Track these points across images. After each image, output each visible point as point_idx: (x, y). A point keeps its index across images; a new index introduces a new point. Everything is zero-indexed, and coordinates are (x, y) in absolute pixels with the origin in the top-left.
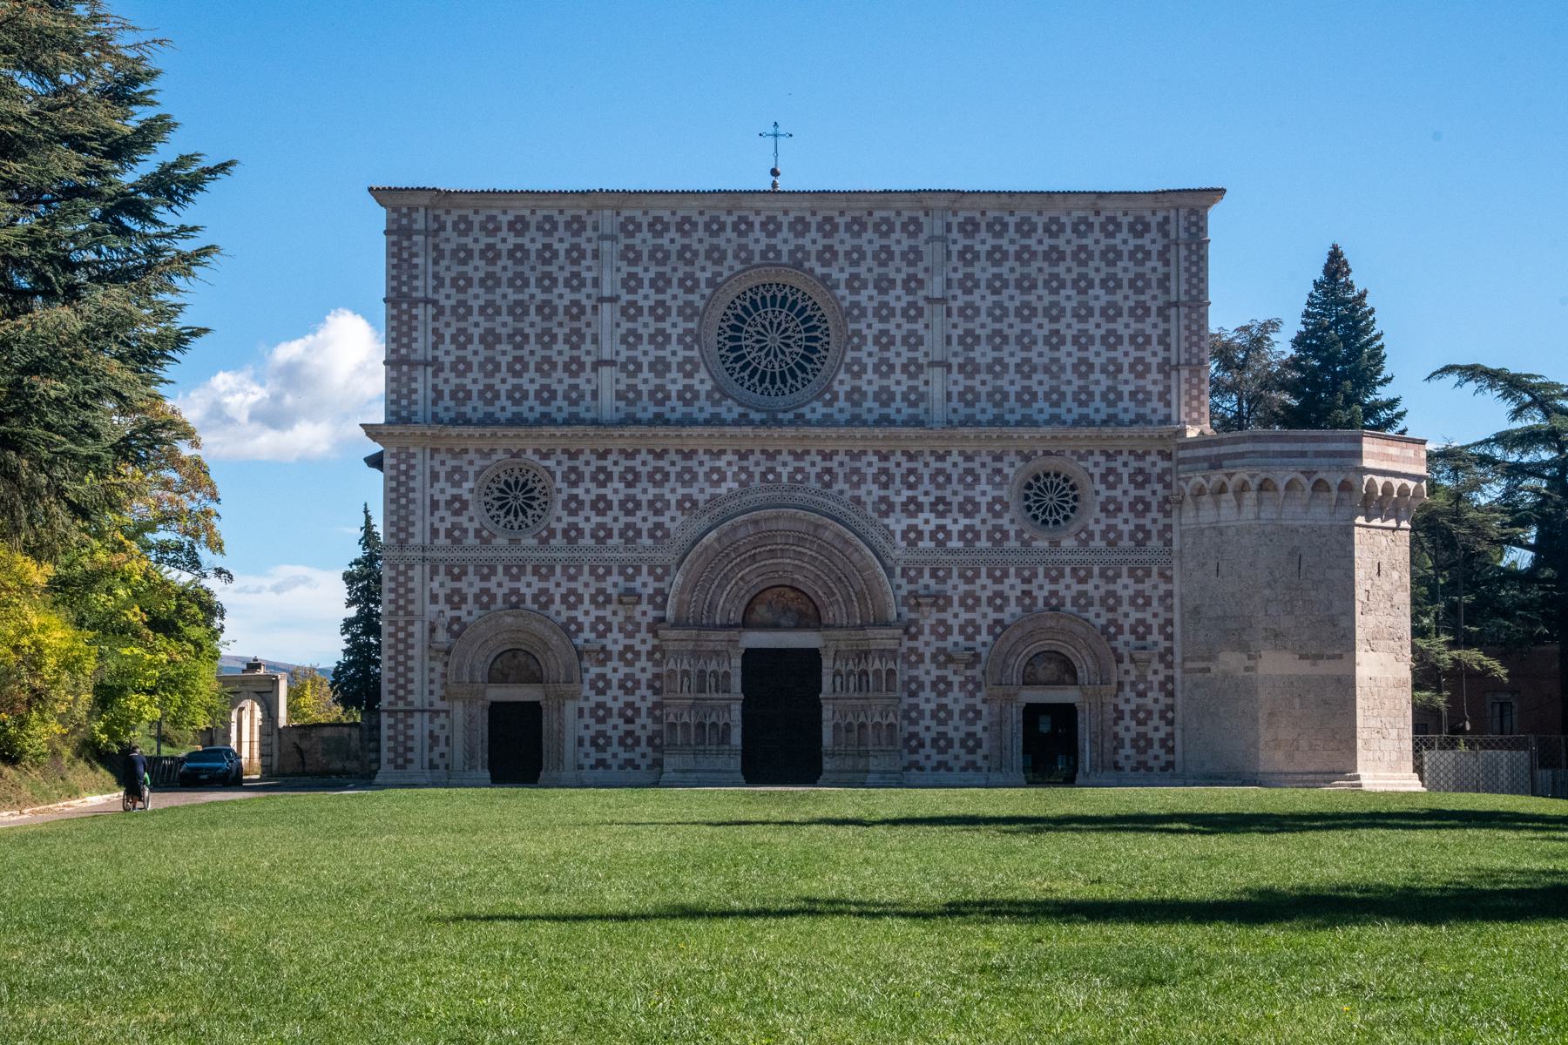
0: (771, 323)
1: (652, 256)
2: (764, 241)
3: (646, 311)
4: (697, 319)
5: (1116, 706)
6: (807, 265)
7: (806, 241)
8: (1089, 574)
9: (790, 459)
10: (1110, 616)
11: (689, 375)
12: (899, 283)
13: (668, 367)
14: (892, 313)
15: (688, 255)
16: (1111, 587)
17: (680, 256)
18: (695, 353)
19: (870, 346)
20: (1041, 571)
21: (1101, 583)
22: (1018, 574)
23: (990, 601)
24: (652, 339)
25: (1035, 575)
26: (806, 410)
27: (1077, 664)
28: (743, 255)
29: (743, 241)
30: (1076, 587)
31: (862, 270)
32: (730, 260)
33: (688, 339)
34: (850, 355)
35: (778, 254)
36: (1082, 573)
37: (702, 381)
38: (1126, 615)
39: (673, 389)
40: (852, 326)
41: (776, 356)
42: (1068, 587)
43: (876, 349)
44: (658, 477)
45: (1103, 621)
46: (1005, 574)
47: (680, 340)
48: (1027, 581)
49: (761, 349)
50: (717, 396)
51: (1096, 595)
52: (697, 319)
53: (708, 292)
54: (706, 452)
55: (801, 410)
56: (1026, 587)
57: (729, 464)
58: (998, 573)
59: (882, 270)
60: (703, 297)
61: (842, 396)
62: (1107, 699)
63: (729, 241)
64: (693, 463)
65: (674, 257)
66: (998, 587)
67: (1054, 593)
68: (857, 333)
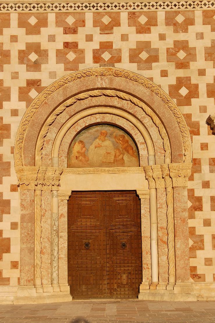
5: (191, 192)
8: (152, 22)
10: (181, 73)
16: (181, 36)
20: (89, 17)
21: (169, 31)
22: (59, 22)
23: (23, 56)
25: (83, 23)
27: (138, 139)
30: (135, 38)
36: (143, 20)
38: (202, 73)
42: (124, 38)
45: (172, 80)
46: (43, 22)
48: (72, 30)
51: (162, 47)
56: (70, 38)
58: (33, 21)
62: (179, 182)
66: (33, 39)
67: (106, 46)
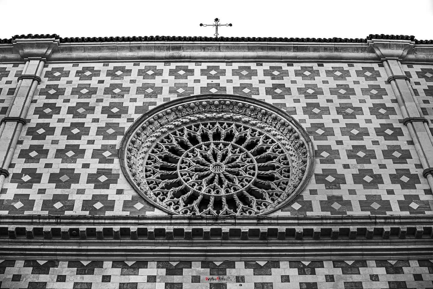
0: (215, 156)
2: (205, 81)
4: (120, 138)
7: (254, 81)
32: (165, 93)
41: (221, 183)
49: (201, 178)
57: (152, 279)
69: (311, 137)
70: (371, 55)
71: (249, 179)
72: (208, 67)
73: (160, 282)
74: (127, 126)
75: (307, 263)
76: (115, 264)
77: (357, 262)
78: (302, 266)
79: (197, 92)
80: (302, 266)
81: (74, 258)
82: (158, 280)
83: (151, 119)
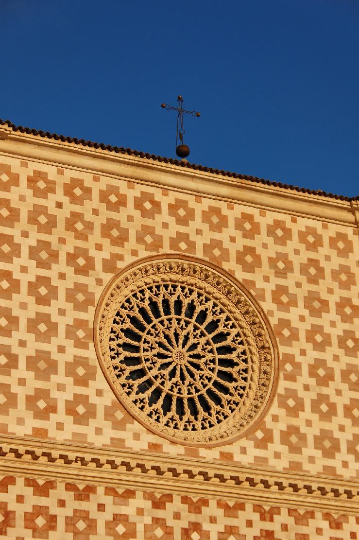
1: (32, 220)
2: (175, 228)
3: (24, 287)
4: (92, 310)
6: (226, 266)
7: (223, 237)
9: (219, 513)
11: (82, 382)
12: (332, 307)
13: (53, 367)
14: (327, 341)
15: (79, 226)
17: (70, 225)
18: (90, 353)
19: (305, 378)
24: (32, 326)
26: (234, 449)
28: (149, 239)
29: (148, 222)
31: (289, 282)
32: (132, 243)
33: (81, 334)
34: (283, 385)
35: (192, 246)
37: (99, 393)
39: (61, 398)
40: (283, 349)
43: (312, 382)
44: (40, 521)
47: (70, 332)
50: (120, 415)
52: (92, 310)
53: (107, 277)
54: (110, 491)
55: (226, 449)
59: (313, 288)
60: (99, 282)
61: (277, 436)
63: (130, 219)
64: (89, 506)
65: (61, 224)
68: (290, 358)
69: (278, 339)
70: (350, 217)
71: (209, 376)
72: (177, 200)
73: (147, 516)
74: (98, 291)
75: (267, 508)
76: (108, 491)
77: (308, 512)
78: (263, 511)
79: (166, 249)
80: (263, 511)
81: (71, 481)
82: (145, 513)
83: (118, 281)
